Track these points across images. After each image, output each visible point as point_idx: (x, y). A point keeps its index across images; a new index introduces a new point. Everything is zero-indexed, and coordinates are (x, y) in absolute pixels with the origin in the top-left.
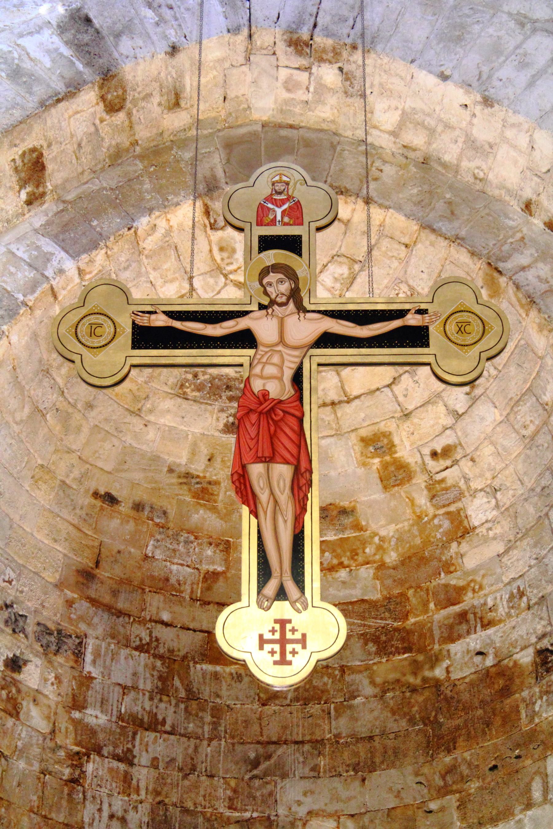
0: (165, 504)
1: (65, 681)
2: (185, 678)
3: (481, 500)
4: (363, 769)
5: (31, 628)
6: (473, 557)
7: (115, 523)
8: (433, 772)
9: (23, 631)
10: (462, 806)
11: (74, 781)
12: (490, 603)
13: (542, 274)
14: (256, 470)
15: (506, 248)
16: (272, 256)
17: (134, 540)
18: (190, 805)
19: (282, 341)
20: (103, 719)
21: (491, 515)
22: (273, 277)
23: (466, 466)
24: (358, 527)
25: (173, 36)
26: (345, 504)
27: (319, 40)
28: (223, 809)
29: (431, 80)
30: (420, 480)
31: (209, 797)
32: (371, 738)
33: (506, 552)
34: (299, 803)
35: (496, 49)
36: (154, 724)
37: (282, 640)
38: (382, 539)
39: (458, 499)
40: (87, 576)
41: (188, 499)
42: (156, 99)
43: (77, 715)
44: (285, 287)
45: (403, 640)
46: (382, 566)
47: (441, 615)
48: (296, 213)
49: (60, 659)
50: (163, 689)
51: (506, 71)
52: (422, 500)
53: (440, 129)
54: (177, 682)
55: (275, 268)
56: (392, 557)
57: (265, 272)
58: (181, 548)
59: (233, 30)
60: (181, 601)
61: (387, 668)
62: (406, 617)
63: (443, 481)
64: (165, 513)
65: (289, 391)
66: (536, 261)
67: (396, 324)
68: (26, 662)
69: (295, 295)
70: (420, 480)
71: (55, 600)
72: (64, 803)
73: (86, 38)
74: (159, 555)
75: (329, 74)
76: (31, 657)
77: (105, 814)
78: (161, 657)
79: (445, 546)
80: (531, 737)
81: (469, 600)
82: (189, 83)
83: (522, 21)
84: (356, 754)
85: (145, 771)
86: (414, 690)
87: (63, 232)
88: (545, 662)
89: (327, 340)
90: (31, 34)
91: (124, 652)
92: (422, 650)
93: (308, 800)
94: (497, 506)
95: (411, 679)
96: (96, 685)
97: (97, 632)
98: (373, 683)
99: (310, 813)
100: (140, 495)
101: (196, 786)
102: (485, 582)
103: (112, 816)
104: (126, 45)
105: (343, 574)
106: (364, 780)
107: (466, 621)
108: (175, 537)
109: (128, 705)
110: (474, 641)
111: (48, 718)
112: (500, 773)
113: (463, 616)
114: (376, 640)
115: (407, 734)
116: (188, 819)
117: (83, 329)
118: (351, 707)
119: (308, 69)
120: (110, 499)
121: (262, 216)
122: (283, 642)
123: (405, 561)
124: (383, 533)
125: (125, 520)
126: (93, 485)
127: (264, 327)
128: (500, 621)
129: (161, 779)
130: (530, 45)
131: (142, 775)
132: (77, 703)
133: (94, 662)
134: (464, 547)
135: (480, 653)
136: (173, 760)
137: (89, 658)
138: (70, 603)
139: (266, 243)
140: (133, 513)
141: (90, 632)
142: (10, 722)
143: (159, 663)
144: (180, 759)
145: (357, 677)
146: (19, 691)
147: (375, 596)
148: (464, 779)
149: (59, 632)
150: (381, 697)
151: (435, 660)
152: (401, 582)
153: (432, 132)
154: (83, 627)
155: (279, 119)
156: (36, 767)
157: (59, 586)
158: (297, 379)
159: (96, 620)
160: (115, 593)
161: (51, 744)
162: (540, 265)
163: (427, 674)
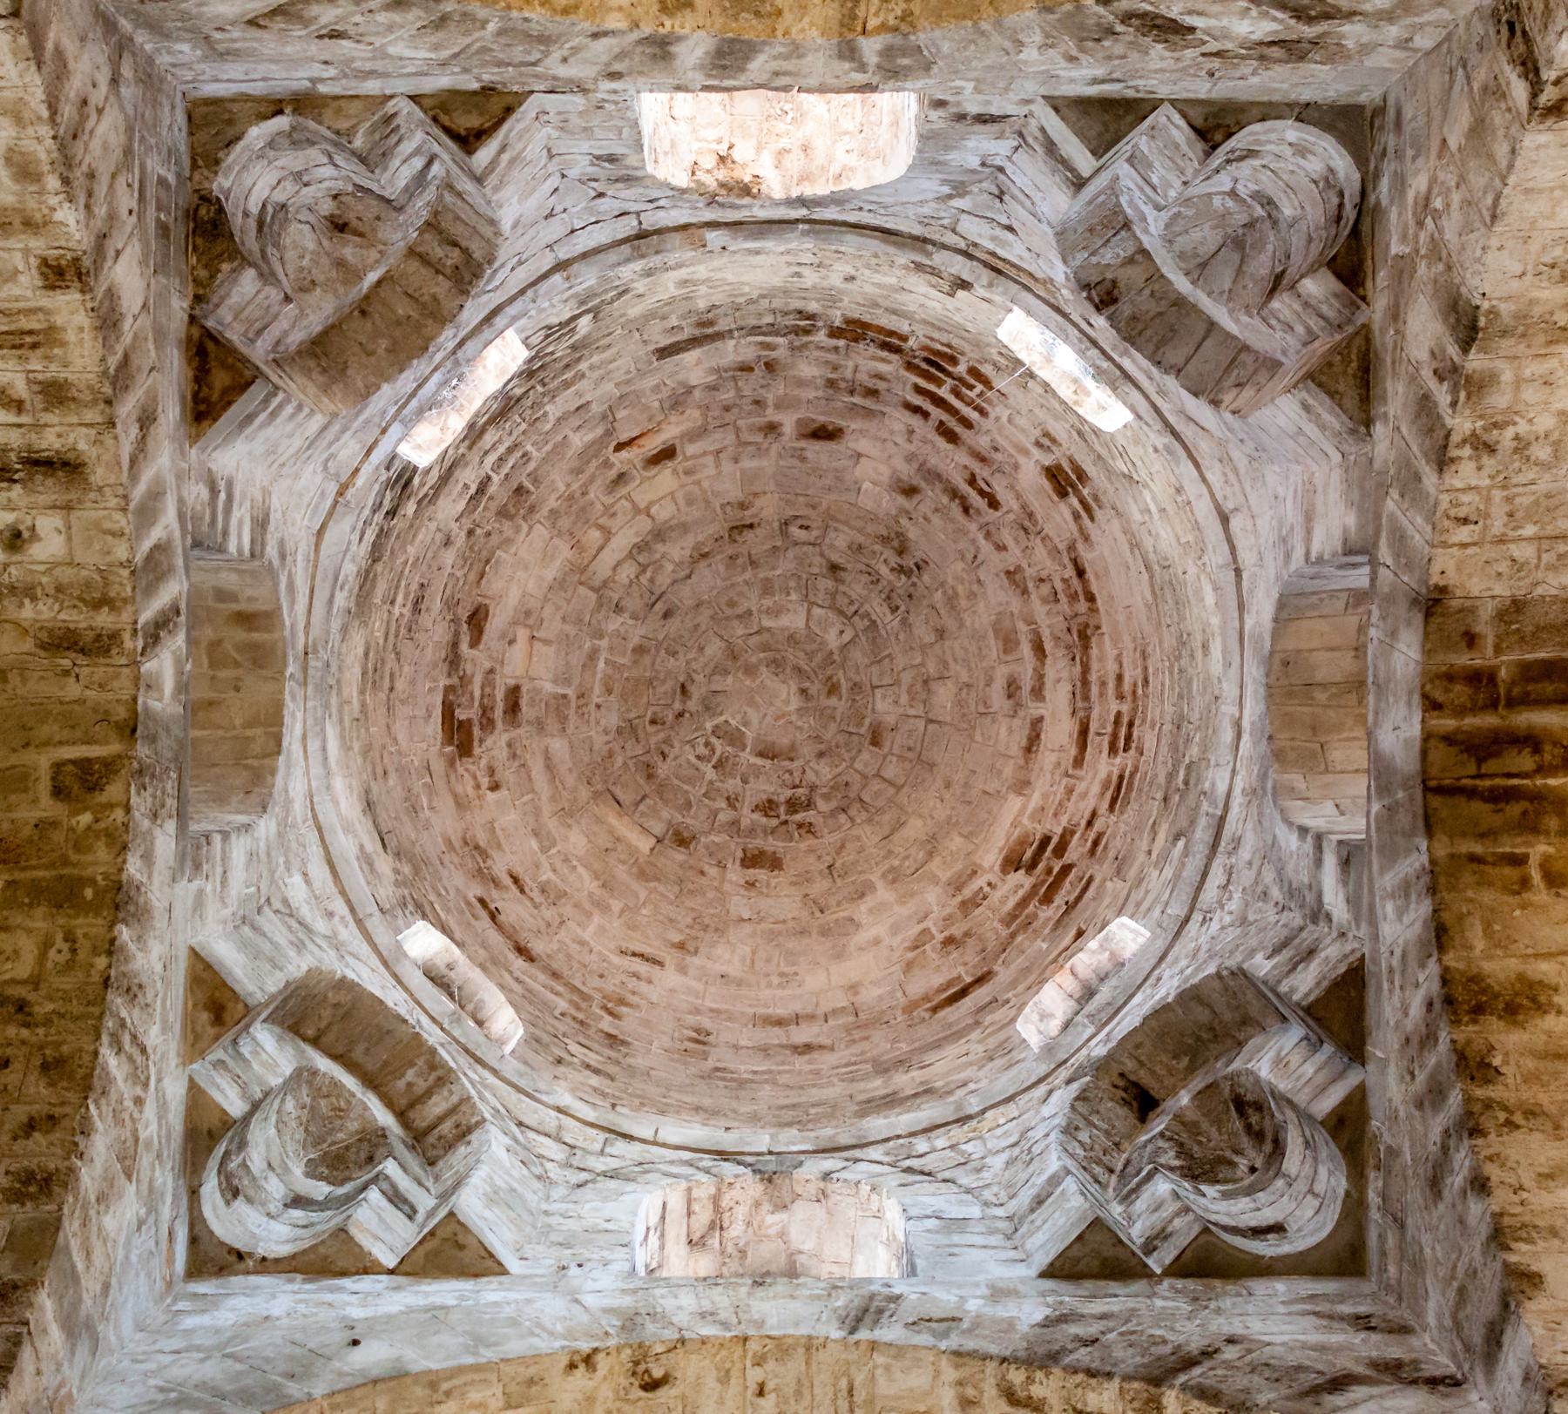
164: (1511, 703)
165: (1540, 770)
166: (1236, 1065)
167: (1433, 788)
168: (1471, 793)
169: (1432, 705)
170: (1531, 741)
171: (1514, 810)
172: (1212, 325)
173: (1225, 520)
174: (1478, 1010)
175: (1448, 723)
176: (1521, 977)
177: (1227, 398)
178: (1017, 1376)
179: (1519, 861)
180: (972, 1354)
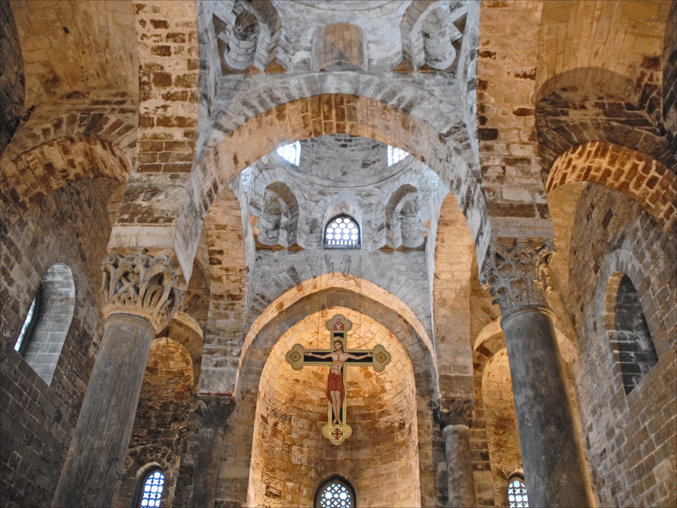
0: (310, 381)
2: (316, 425)
6: (386, 397)
14: (332, 392)
16: (337, 338)
19: (339, 360)
20: (296, 436)
22: (337, 344)
23: (385, 375)
24: (358, 387)
25: (315, 274)
28: (324, 458)
29: (376, 287)
30: (374, 377)
35: (392, 279)
36: (307, 437)
40: (292, 400)
44: (340, 346)
46: (364, 397)
47: (378, 411)
48: (342, 327)
50: (310, 429)
51: (394, 285)
52: (374, 382)
55: (337, 341)
56: (367, 395)
57: (335, 342)
59: (329, 272)
65: (340, 372)
67: (365, 356)
69: (342, 348)
70: (374, 377)
71: (284, 407)
74: (309, 394)
75: (352, 282)
79: (380, 394)
80: (397, 444)
81: (385, 408)
82: (318, 284)
83: (399, 272)
89: (349, 360)
96: (294, 428)
97: (294, 413)
100: (305, 379)
105: (355, 399)
110: (385, 419)
117: (293, 356)
120: (298, 381)
121: (335, 328)
122: (337, 434)
123: (370, 397)
125: (302, 385)
126: (293, 378)
127: (334, 357)
129: (310, 451)
130: (400, 278)
131: (305, 449)
132: (289, 433)
138: (288, 407)
139: (336, 335)
147: (362, 405)
158: (342, 370)
160: (299, 404)
164: (337, 109)
165: (324, 113)
166: (261, 24)
167: (320, 97)
168: (320, 102)
169: (336, 95)
170: (330, 110)
171: (317, 109)
172: (422, 12)
173: (380, 7)
174: (278, 111)
175: (333, 97)
176: (285, 116)
177: (405, 19)
178: (195, 35)
179: (307, 111)
180: (198, 25)
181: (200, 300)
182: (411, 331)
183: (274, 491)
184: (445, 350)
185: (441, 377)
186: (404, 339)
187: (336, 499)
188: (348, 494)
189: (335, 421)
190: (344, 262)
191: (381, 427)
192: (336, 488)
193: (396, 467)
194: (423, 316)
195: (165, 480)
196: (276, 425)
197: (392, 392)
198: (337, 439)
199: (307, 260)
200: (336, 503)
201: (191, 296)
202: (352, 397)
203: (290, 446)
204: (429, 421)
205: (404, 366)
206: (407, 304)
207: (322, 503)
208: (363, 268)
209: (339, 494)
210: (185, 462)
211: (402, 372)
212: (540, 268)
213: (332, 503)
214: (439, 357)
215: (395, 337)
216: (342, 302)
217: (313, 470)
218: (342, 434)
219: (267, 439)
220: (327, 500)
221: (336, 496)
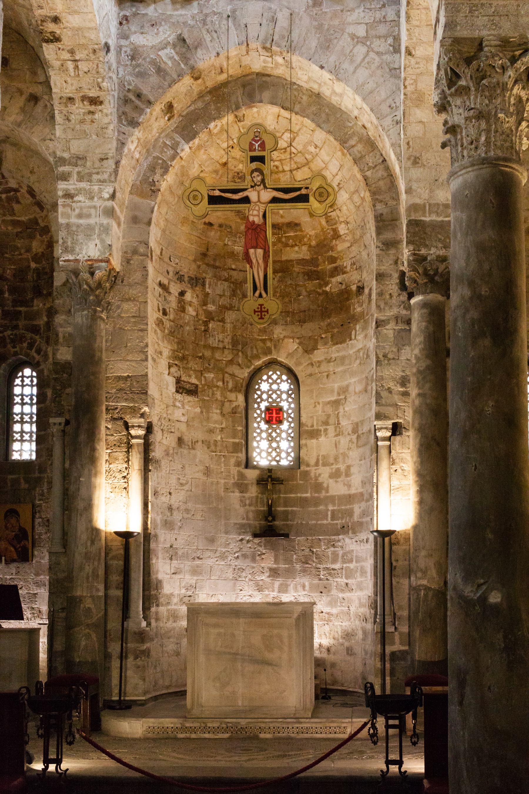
1: (200, 296)
3: (343, 226)
4: (302, 322)
5: (186, 279)
6: (341, 246)
7: (212, 234)
8: (323, 324)
9: (184, 281)
10: (332, 337)
11: (205, 331)
12: (345, 265)
13: (359, 149)
15: (347, 137)
17: (220, 239)
18: (245, 335)
20: (213, 308)
21: (346, 232)
23: (338, 211)
24: (301, 230)
26: (297, 222)
27: (274, 48)
29: (318, 68)
31: (251, 332)
32: (305, 311)
33: (351, 246)
34: (281, 333)
36: (231, 308)
37: (261, 311)
38: (310, 236)
39: (335, 224)
41: (239, 220)
42: (213, 72)
43: (205, 308)
45: (317, 275)
46: (310, 246)
49: (197, 288)
50: (234, 294)
52: (323, 222)
53: (322, 84)
54: (238, 292)
56: (313, 243)
58: (238, 240)
60: (238, 260)
61: (311, 285)
62: (318, 266)
63: (330, 216)
64: (231, 227)
66: (357, 143)
68: (185, 292)
72: (203, 338)
73: (184, 50)
74: (230, 243)
76: (187, 290)
77: (217, 341)
78: (233, 283)
79: (331, 241)
84: (300, 317)
85: (229, 325)
86: (319, 294)
87: (182, 131)
88: (359, 291)
90: (163, 49)
91: (219, 283)
92: (323, 280)
93: (284, 332)
94: (348, 229)
95: (320, 291)
96: (210, 296)
97: (209, 277)
98: (306, 291)
99: (284, 337)
100: (221, 221)
101: (247, 328)
102: (344, 256)
103: (219, 341)
104: (200, 53)
105: (296, 248)
106: (302, 326)
107: (337, 271)
108: (235, 236)
109: (222, 301)
110: (339, 278)
111: (195, 310)
112: (345, 327)
113: (336, 268)
114: (308, 275)
115: (316, 311)
116: (244, 339)
118: (299, 300)
119: (271, 56)
120: (210, 224)
122: (261, 312)
123: (318, 245)
124: (310, 233)
128: (347, 273)
129: (235, 327)
131: (228, 326)
132: (205, 304)
133: (209, 288)
134: (338, 242)
135: (341, 283)
136: (238, 320)
137: (207, 286)
138: (199, 267)
140: (219, 228)
141: (207, 276)
142: (182, 315)
143: (232, 285)
144: (241, 320)
145: (301, 288)
146: (184, 303)
147: (308, 258)
148: (334, 328)
149: (196, 278)
150: (309, 296)
151: (327, 284)
152: (316, 253)
153: (320, 85)
154: (204, 275)
155: (263, 72)
156: (193, 328)
157: (195, 261)
159: (209, 271)
160: (215, 260)
161: (196, 319)
162: (359, 145)
163: (324, 289)
181: (41, 104)
182: (371, 145)
183: (187, 386)
184: (418, 180)
185: (411, 223)
186: (362, 157)
187: (275, 392)
188: (291, 384)
189: (257, 294)
190: (264, 22)
191: (333, 290)
192: (275, 377)
193: (352, 348)
194: (388, 121)
195: (37, 377)
196: (182, 294)
197: (348, 238)
198: (261, 318)
199: (204, 23)
200: (274, 396)
201: (24, 97)
202: (292, 246)
203: (206, 323)
204: (393, 285)
205: (363, 199)
206: (364, 99)
207: (256, 396)
208: (295, 35)
209: (278, 384)
210: (59, 356)
211: (361, 209)
212: (515, 91)
213: (270, 396)
214: (409, 191)
215: (348, 156)
216: (266, 95)
217: (240, 354)
218: (267, 311)
219: (172, 317)
220: (262, 393)
221: (275, 387)
